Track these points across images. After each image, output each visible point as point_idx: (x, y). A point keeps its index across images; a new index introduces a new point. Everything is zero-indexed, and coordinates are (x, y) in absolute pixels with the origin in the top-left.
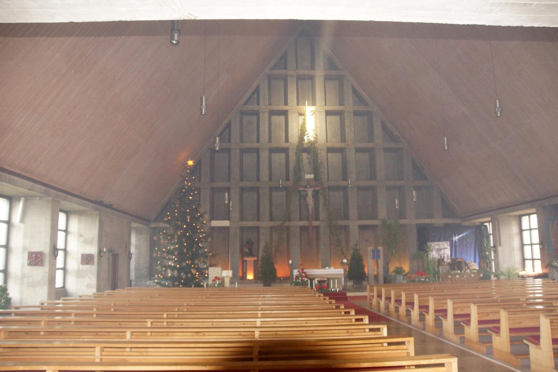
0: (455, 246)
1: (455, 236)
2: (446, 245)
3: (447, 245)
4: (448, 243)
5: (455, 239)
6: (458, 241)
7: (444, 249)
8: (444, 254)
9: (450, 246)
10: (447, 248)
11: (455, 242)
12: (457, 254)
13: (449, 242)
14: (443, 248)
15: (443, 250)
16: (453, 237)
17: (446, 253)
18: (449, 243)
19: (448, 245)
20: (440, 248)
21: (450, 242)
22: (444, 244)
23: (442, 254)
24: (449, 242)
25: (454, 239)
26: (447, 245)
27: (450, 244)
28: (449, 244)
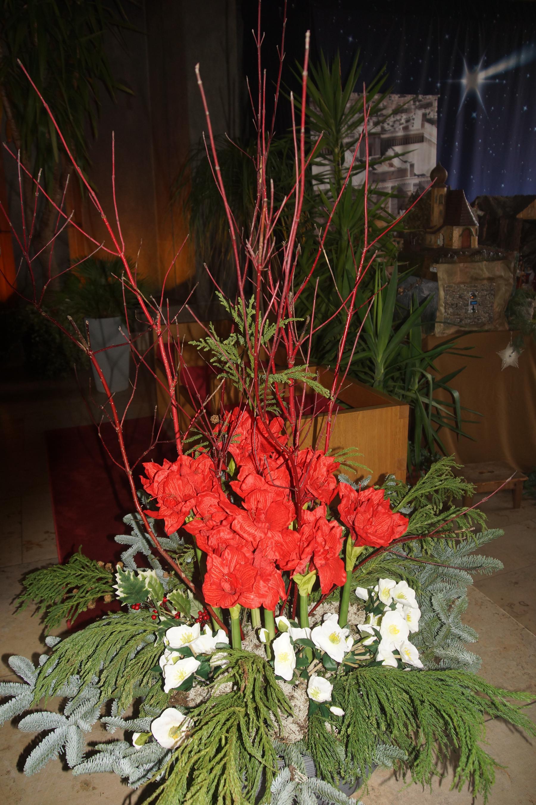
0: (470, 123)
1: (472, 64)
2: (420, 113)
3: (426, 119)
4: (429, 105)
5: (473, 80)
6: (483, 97)
7: (407, 140)
8: (401, 173)
9: (438, 123)
10: (420, 139)
11: (472, 96)
12: (475, 179)
13: (433, 99)
14: (400, 133)
15: (398, 149)
16: (459, 74)
17: (416, 172)
18: (436, 104)
19: (431, 121)
20: (384, 136)
21: (439, 106)
22: (406, 111)
23: (392, 169)
24: (433, 99)
25: (464, 81)
26: (426, 119)
27: (439, 112)
28: (433, 115)
